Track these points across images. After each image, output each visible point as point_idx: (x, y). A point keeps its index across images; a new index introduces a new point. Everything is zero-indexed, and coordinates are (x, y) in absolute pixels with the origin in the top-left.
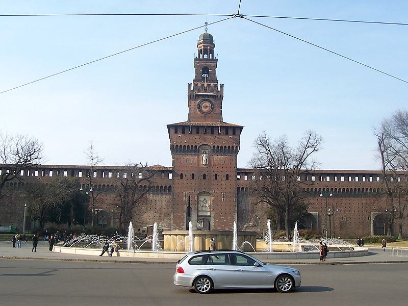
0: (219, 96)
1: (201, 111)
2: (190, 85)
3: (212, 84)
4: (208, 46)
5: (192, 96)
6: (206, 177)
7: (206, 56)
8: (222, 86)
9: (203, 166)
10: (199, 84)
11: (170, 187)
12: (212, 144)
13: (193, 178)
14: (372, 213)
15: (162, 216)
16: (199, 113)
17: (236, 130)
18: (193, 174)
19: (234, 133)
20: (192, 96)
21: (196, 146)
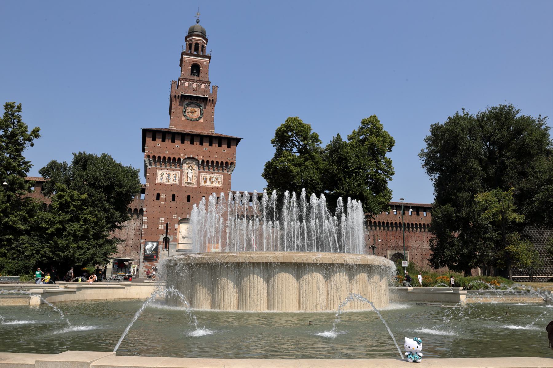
0: (211, 100)
1: (185, 116)
2: (173, 83)
3: (203, 86)
4: (200, 40)
5: (177, 96)
6: (191, 199)
7: (195, 53)
8: (215, 88)
9: (188, 186)
10: (187, 84)
11: (142, 210)
12: (200, 158)
13: (173, 199)
14: (388, 251)
15: (128, 249)
16: (184, 118)
17: (232, 142)
18: (174, 196)
19: (229, 146)
20: (177, 96)
21: (179, 159)
